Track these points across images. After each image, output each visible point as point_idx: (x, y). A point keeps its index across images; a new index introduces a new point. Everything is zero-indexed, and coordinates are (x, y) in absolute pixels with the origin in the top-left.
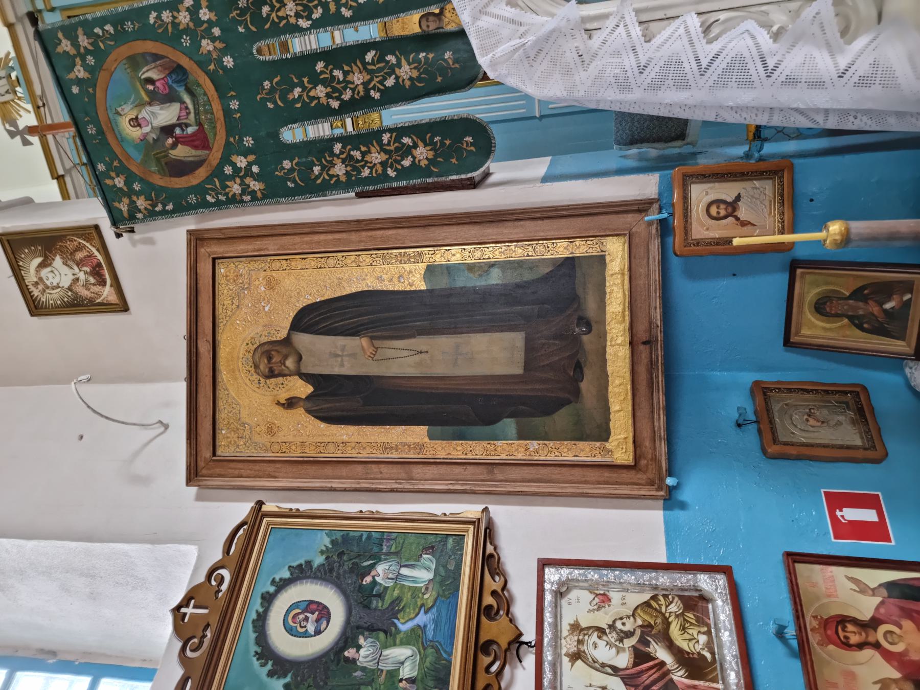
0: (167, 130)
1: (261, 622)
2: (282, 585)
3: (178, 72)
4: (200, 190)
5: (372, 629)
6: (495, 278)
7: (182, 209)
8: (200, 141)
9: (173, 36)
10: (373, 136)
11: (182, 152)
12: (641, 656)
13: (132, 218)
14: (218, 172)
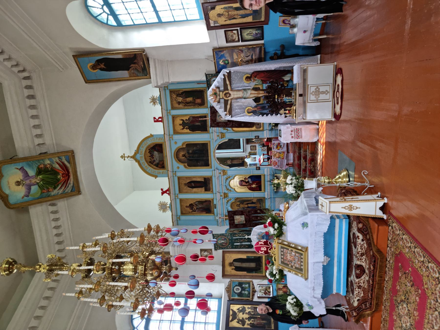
0: (223, 243)
1: (233, 290)
2: (235, 287)
3: (226, 239)
4: (225, 248)
5: (243, 290)
6: (253, 258)
7: (222, 249)
8: (226, 244)
9: (226, 236)
10: (243, 245)
11: (224, 244)
12: (265, 291)
13: (217, 249)
14: (227, 246)
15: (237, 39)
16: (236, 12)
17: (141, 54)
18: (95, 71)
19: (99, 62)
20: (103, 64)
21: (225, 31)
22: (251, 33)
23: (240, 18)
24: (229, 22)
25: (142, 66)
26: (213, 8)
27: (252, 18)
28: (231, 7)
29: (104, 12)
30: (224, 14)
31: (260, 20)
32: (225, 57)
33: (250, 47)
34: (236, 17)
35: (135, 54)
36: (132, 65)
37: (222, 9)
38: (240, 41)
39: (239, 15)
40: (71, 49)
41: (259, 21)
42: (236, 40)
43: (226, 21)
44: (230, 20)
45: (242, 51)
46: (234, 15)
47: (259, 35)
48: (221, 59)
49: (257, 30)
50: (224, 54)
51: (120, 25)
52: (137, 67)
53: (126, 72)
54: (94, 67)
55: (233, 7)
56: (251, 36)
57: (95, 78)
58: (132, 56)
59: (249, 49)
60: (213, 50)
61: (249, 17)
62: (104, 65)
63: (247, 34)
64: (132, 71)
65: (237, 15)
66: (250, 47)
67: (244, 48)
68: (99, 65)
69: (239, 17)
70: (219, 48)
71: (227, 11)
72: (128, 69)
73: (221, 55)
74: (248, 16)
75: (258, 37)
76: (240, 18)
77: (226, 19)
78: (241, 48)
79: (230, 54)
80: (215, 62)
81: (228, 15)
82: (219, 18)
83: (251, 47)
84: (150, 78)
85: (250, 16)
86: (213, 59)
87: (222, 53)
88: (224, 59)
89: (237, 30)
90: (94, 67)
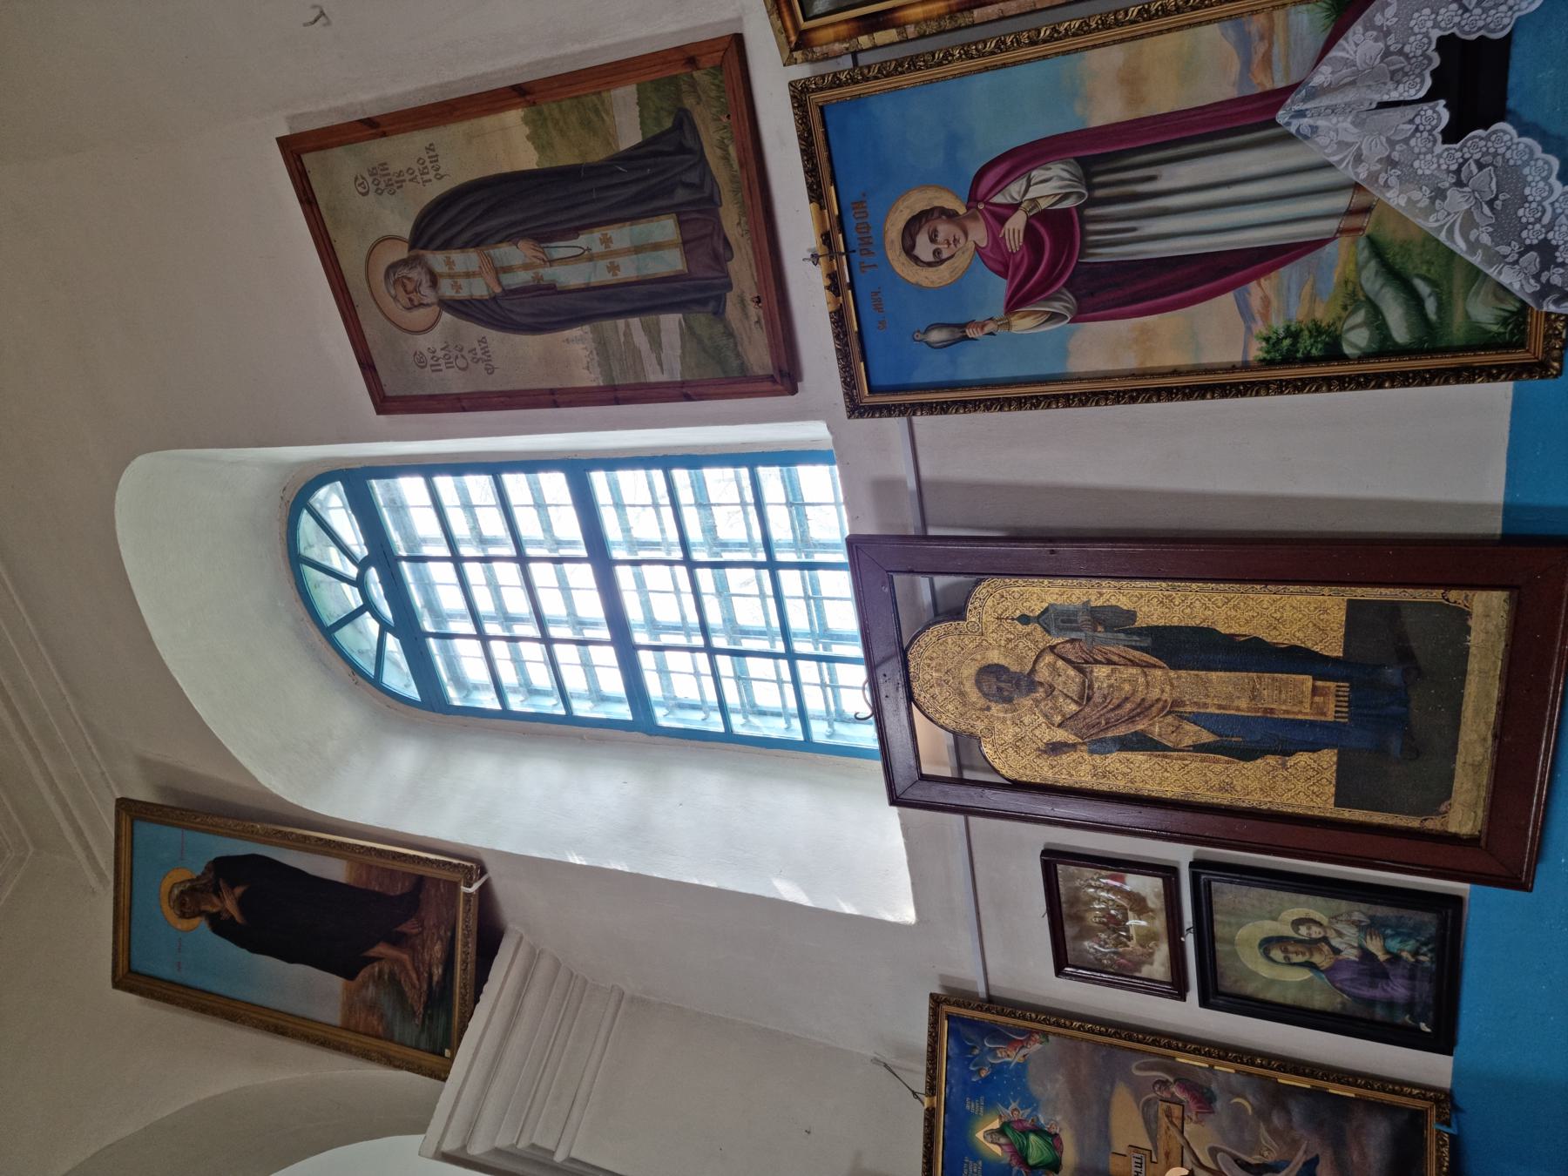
15: (1158, 968)
16: (1162, 682)
17: (456, 885)
18: (184, 924)
19: (225, 869)
20: (239, 891)
21: (1052, 859)
22: (1312, 944)
23: (1200, 748)
24: (1081, 769)
25: (438, 972)
26: (951, 610)
27: (1330, 774)
28: (1116, 621)
29: (368, 606)
30: (1043, 674)
31: (1433, 824)
32: (1029, 1101)
33: (1285, 1080)
34: (1157, 728)
35: (420, 880)
36: (381, 949)
37: (1024, 619)
38: (1193, 995)
39: (1196, 719)
40: (144, 763)
41: (1414, 823)
42: (1145, 971)
43: (1055, 748)
44: (1100, 746)
45: (1204, 1099)
46: (1143, 709)
47: (1398, 990)
48: (989, 1105)
49: (1372, 927)
50: (1022, 1068)
51: (432, 699)
52: (403, 967)
53: (336, 983)
54: (189, 900)
55: (1131, 615)
56: (1304, 975)
57: (166, 971)
58: (399, 889)
59: (1279, 1097)
60: (936, 1000)
61: (1303, 758)
62: (241, 903)
63: (1267, 944)
64: (371, 991)
65: (1173, 709)
66: (1285, 1080)
67: (1223, 1068)
68: (217, 891)
69: (1187, 741)
70: (992, 1002)
71: (1071, 652)
72: (348, 973)
73: (998, 1070)
74: (1286, 751)
75: (1390, 1004)
76: (1200, 748)
77: (1061, 735)
78: (1200, 1063)
79: (1075, 1089)
80: (931, 1114)
81: (1085, 697)
82: (996, 709)
83: (1305, 1083)
84: (441, 1075)
85: (1314, 748)
86: (920, 1084)
87: (1013, 1057)
88: (1013, 1111)
89: (1167, 873)
90: (189, 900)
